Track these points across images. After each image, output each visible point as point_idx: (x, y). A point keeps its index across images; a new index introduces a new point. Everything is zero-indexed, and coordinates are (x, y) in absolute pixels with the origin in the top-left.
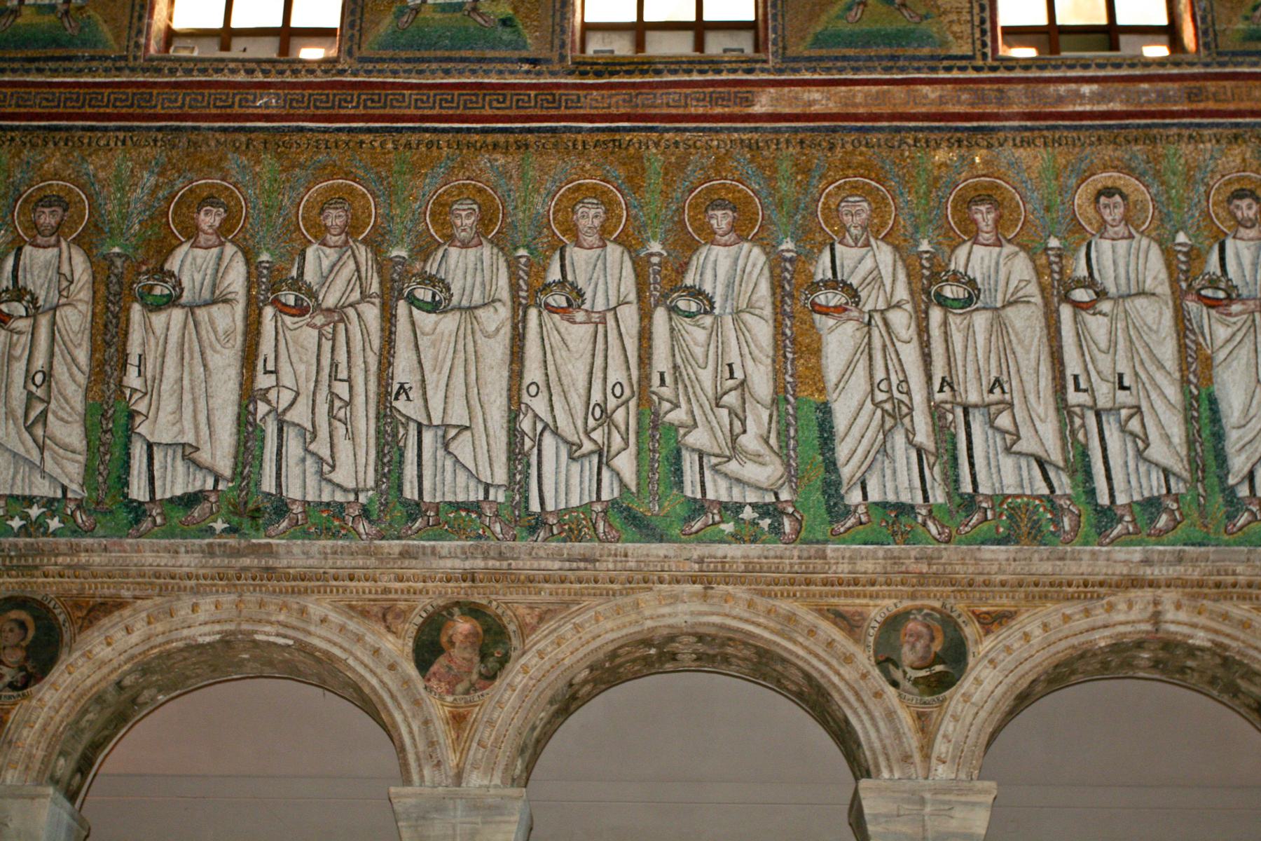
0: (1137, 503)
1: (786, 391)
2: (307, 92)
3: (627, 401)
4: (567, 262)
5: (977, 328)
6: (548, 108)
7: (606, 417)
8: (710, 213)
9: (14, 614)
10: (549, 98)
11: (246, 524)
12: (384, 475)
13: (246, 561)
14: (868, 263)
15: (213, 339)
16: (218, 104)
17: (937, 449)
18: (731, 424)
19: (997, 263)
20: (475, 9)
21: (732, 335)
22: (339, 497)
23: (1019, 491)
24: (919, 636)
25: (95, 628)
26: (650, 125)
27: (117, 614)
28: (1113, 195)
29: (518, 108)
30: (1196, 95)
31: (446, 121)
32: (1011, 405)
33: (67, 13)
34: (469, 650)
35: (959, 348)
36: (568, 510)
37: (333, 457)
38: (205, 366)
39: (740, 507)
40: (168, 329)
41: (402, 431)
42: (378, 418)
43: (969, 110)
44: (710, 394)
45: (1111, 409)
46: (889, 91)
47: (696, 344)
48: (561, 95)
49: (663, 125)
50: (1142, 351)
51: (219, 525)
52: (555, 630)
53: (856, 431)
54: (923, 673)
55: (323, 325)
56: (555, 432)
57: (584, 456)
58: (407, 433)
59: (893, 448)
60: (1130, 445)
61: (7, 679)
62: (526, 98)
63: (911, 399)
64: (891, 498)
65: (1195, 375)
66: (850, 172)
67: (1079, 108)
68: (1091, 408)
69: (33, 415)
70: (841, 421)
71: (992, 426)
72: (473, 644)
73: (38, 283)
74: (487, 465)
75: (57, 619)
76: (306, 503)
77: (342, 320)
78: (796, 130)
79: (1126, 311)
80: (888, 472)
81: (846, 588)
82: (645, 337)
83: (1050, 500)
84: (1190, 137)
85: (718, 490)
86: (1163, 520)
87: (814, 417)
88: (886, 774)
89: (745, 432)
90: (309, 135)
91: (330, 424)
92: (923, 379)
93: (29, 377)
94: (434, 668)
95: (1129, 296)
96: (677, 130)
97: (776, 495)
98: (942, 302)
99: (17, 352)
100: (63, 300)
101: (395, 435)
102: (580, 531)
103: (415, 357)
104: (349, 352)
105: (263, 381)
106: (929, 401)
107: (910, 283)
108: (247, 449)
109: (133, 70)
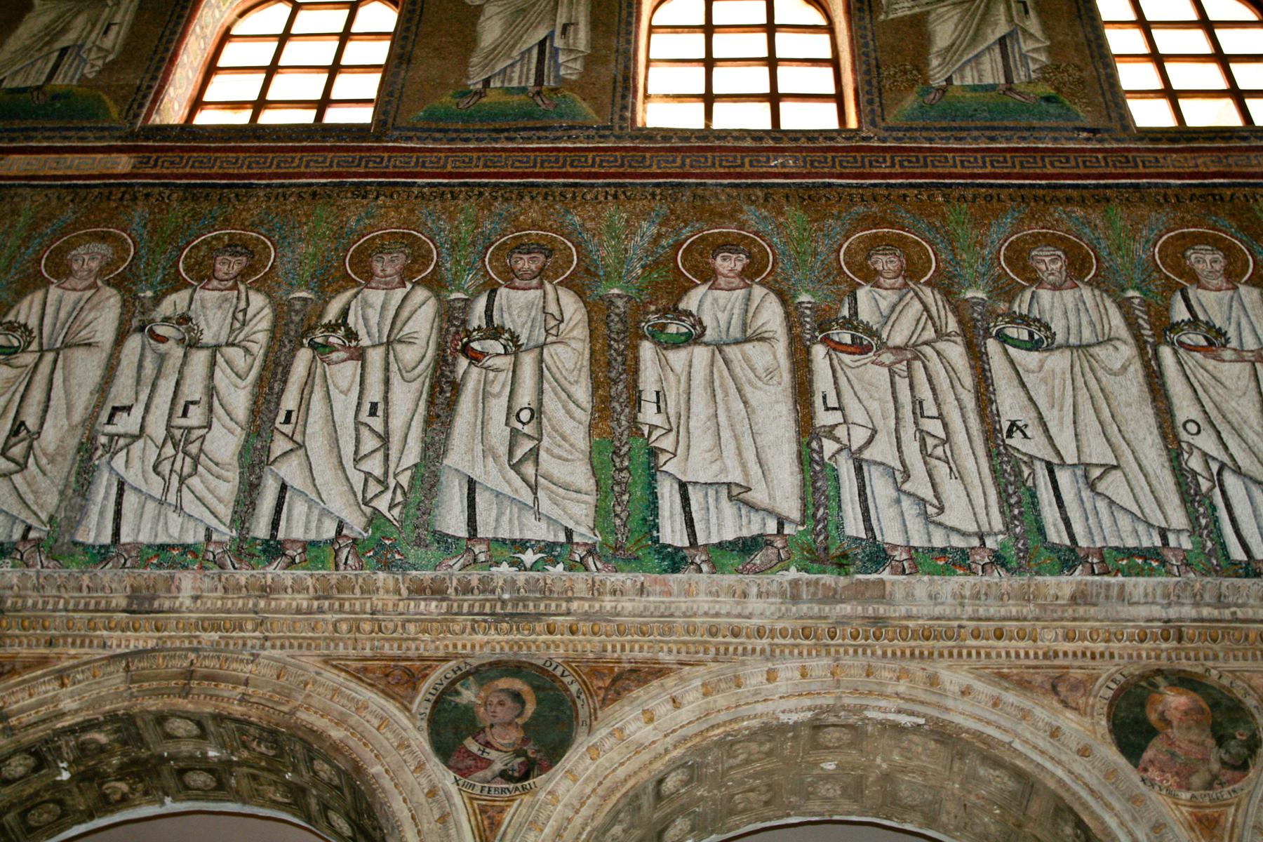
9: (503, 683)
10: (1123, 160)
15: (751, 375)
20: (1010, 89)
22: (957, 541)
25: (625, 701)
27: (655, 683)
33: (539, 93)
37: (937, 496)
38: (745, 403)
40: (690, 366)
41: (1026, 471)
56: (1238, 471)
58: (1033, 473)
61: (498, 767)
69: (519, 454)
72: (1198, 723)
73: (519, 321)
74: (1155, 506)
75: (567, 690)
76: (910, 548)
77: (916, 358)
91: (926, 463)
93: (512, 412)
94: (1149, 754)
99: (495, 389)
100: (550, 339)
103: (1022, 394)
105: (824, 418)
108: (816, 490)
109: (619, 138)
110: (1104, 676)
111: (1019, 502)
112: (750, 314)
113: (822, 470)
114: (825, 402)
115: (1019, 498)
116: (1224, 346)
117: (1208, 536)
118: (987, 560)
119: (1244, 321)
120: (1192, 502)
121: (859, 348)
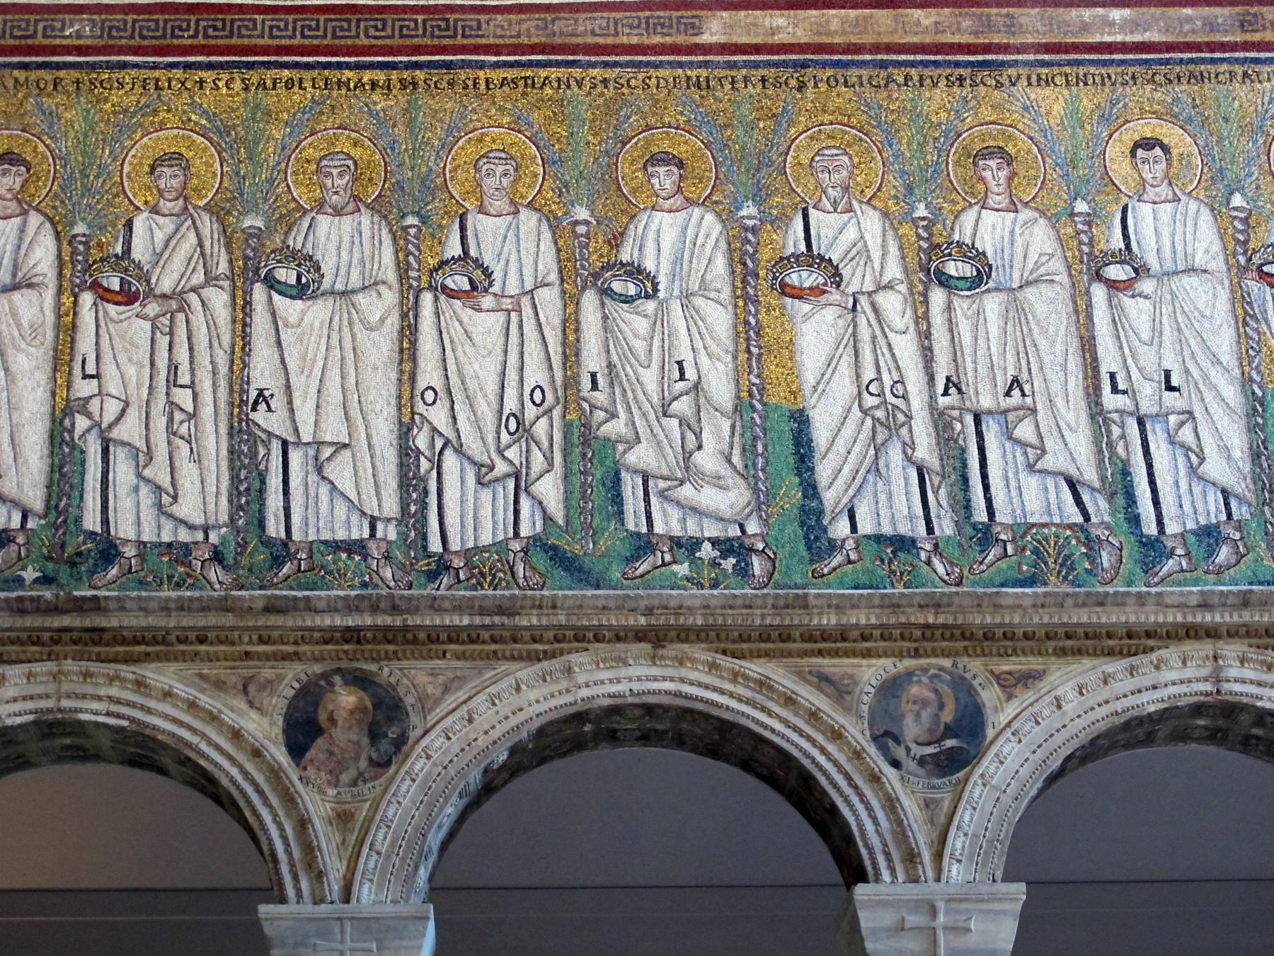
0: (1194, 532)
1: (751, 395)
2: (130, 18)
3: (550, 410)
4: (470, 233)
5: (989, 315)
6: (438, 37)
7: (523, 430)
8: (650, 169)
10: (443, 24)
11: (64, 573)
12: (241, 508)
13: (66, 621)
14: (851, 233)
15: (16, 334)
16: (16, 33)
17: (943, 466)
18: (683, 439)
19: (1012, 232)
21: (681, 325)
22: (184, 536)
23: (1045, 519)
24: (924, 703)
26: (570, 58)
28: (1153, 148)
29: (402, 36)
30: (1251, 24)
31: (309, 55)
32: (1034, 411)
34: (356, 730)
35: (966, 339)
36: (478, 549)
37: (173, 484)
39: (693, 545)
41: (262, 451)
42: (231, 435)
43: (971, 40)
44: (655, 400)
45: (1157, 415)
46: (871, 17)
47: (636, 336)
48: (456, 21)
49: (587, 58)
50: (1192, 342)
51: (30, 574)
52: (465, 702)
53: (840, 446)
54: (930, 750)
55: (158, 316)
57: (497, 480)
58: (268, 454)
59: (887, 466)
60: (1181, 460)
62: (412, 24)
63: (909, 404)
64: (887, 530)
65: (1259, 372)
66: (826, 118)
67: (1108, 39)
68: (1131, 414)
70: (821, 434)
71: (1010, 438)
72: (360, 722)
74: (373, 492)
76: (141, 544)
77: (181, 309)
78: (756, 65)
79: (1174, 295)
80: (883, 497)
81: (833, 645)
82: (571, 325)
83: (1083, 530)
84: (1245, 75)
85: (667, 522)
86: (1224, 553)
87: (787, 427)
88: (886, 876)
89: (700, 447)
90: (133, 72)
92: (923, 378)
94: (308, 755)
95: (1176, 273)
96: (606, 65)
97: (742, 527)
98: (945, 281)
101: (253, 454)
102: (494, 576)
103: (276, 356)
104: (191, 349)
106: (930, 406)
107: (903, 258)
108: (63, 475)
110: (290, 676)
111: (247, 490)
112: (23, 252)
113: (70, 453)
114: (83, 368)
115: (249, 484)
116: (486, 291)
117: (413, 525)
118: (207, 556)
119: (513, 258)
120: (409, 485)
121: (127, 297)
